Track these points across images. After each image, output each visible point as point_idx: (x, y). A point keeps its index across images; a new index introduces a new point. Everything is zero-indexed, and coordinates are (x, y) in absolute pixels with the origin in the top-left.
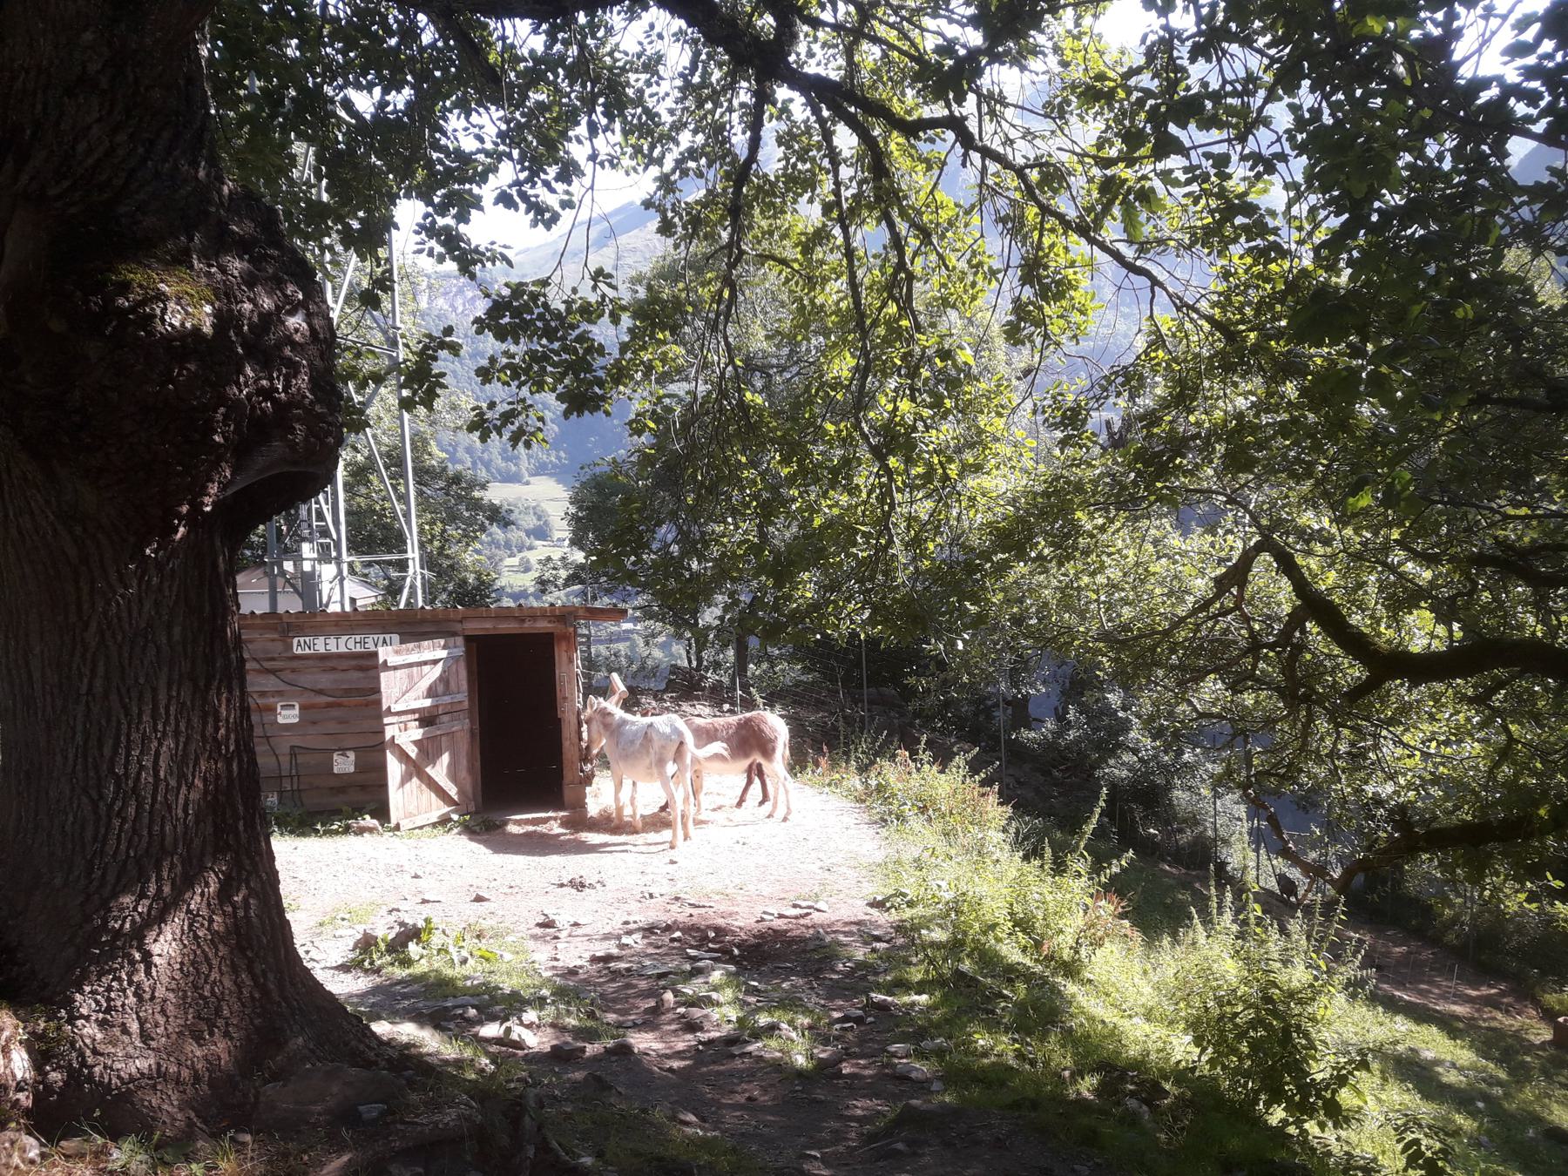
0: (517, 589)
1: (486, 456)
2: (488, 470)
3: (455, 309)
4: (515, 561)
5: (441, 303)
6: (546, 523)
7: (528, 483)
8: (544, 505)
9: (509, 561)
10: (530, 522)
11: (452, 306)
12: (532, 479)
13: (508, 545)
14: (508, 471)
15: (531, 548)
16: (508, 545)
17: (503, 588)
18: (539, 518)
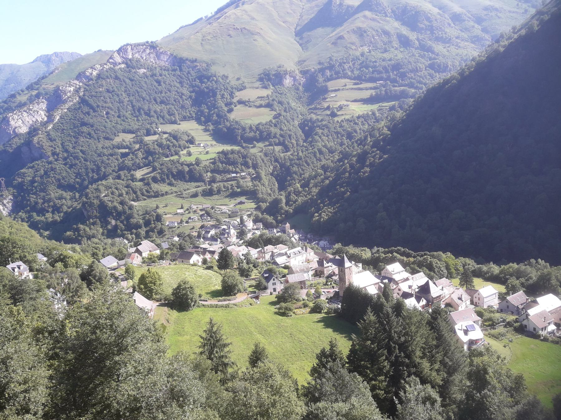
0: (188, 162)
1: (162, 114)
2: (163, 120)
3: (142, 58)
4: (185, 152)
5: (137, 55)
6: (193, 138)
7: (180, 124)
8: (189, 132)
9: (182, 153)
10: (186, 138)
11: (141, 57)
12: (181, 122)
13: (180, 147)
14: (171, 120)
15: (188, 147)
16: (180, 147)
17: (183, 162)
18: (188, 136)
